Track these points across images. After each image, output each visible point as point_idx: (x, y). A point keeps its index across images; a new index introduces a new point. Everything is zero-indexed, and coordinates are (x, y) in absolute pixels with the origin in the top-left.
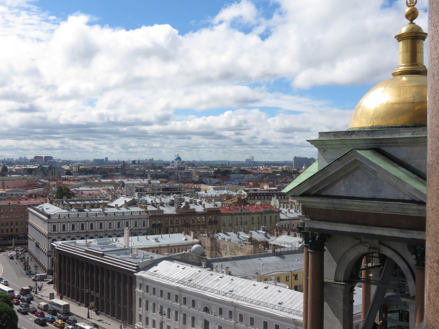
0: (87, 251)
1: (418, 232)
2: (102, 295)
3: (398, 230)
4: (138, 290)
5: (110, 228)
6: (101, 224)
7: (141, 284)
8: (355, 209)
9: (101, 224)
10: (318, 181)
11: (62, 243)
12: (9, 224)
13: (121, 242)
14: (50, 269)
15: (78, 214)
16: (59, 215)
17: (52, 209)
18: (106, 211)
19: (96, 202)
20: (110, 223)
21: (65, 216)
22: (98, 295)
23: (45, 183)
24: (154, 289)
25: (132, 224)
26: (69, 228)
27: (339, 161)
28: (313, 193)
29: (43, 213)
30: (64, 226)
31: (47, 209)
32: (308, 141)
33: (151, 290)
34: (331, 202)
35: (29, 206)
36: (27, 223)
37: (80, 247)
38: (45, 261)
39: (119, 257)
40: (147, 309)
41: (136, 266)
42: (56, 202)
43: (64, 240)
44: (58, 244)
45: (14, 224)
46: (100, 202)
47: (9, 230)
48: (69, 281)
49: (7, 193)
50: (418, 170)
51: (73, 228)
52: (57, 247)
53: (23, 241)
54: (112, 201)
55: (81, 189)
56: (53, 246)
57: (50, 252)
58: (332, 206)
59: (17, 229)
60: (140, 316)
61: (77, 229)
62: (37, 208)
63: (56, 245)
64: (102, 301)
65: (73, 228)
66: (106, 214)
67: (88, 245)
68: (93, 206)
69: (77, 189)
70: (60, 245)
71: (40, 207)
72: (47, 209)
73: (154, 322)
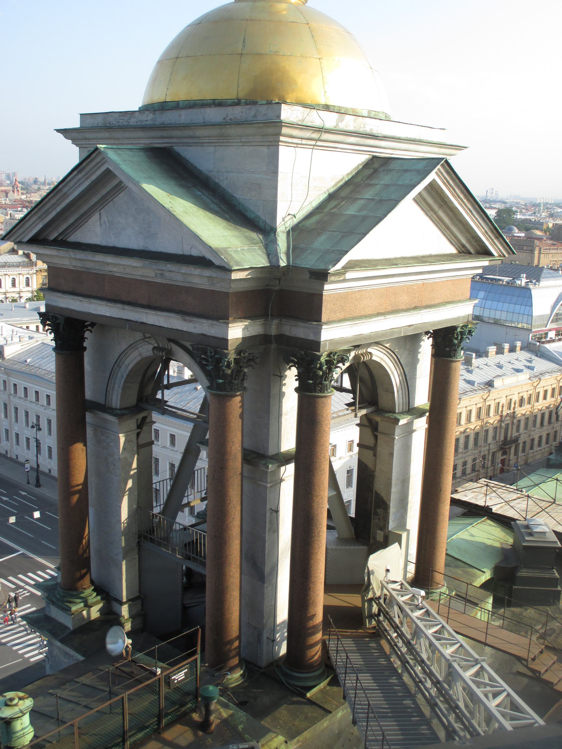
1: (210, 322)
3: (179, 317)
8: (117, 271)
10: (54, 214)
24: (26, 389)
27: (79, 172)
28: (52, 238)
32: (58, 131)
33: (21, 392)
34: (73, 256)
50: (232, 196)
58: (80, 265)
73: (28, 439)
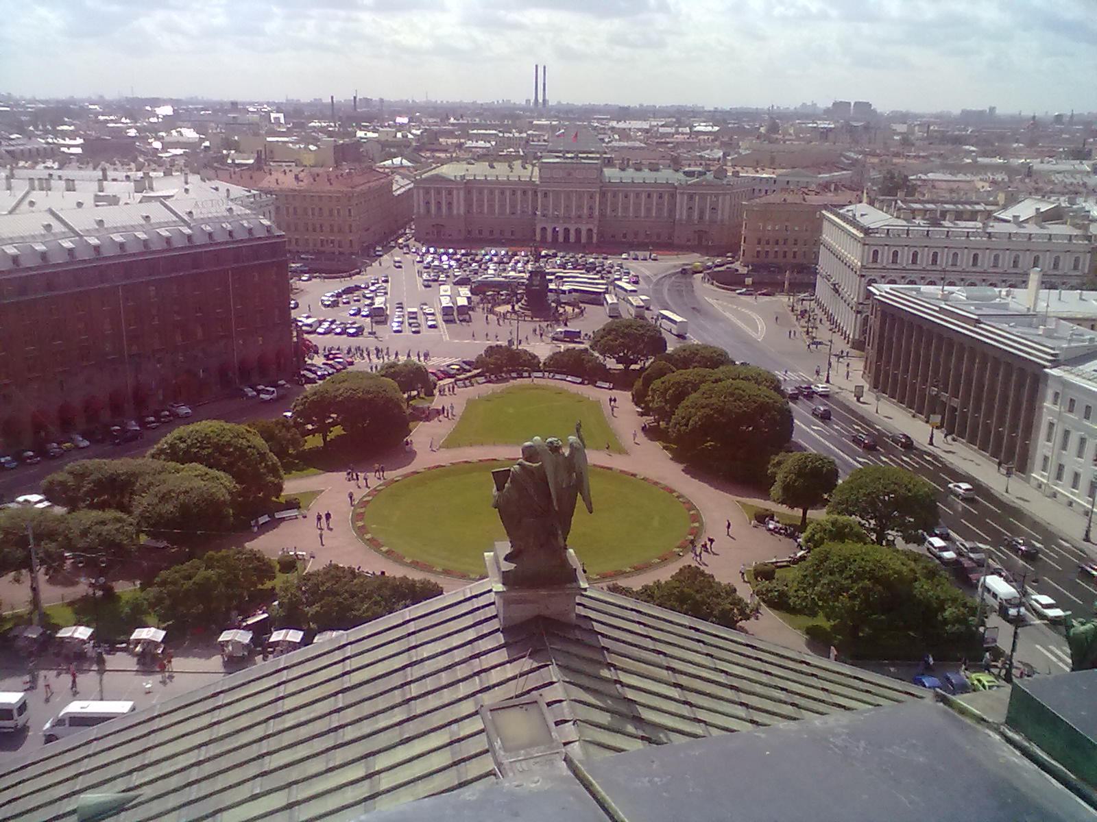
0: (942, 310)
2: (965, 404)
4: (1047, 404)
5: (995, 266)
6: (975, 257)
7: (1057, 395)
9: (975, 257)
11: (891, 289)
12: (781, 242)
13: (1020, 299)
14: (857, 337)
15: (928, 231)
16: (888, 230)
17: (875, 217)
18: (989, 230)
19: (968, 207)
20: (996, 257)
21: (900, 232)
22: (956, 402)
23: (857, 160)
25: (1047, 261)
26: (905, 258)
29: (853, 222)
30: (895, 254)
31: (862, 215)
35: (825, 207)
36: (817, 243)
37: (928, 299)
38: (849, 322)
39: (1014, 331)
40: (1064, 447)
41: (1052, 355)
42: (882, 201)
43: (894, 282)
44: (882, 290)
45: (791, 241)
46: (977, 207)
47: (781, 255)
48: (897, 366)
49: (781, 178)
51: (914, 261)
52: (880, 295)
53: (805, 278)
54: (1005, 207)
55: (931, 176)
56: (870, 295)
57: (861, 304)
59: (795, 253)
60: (1046, 459)
61: (922, 261)
62: (841, 211)
63: (877, 293)
64: (964, 415)
65: (914, 261)
66: (990, 235)
67: (945, 298)
68: (959, 216)
69: (924, 177)
70: (886, 292)
71: (848, 211)
72: (862, 215)
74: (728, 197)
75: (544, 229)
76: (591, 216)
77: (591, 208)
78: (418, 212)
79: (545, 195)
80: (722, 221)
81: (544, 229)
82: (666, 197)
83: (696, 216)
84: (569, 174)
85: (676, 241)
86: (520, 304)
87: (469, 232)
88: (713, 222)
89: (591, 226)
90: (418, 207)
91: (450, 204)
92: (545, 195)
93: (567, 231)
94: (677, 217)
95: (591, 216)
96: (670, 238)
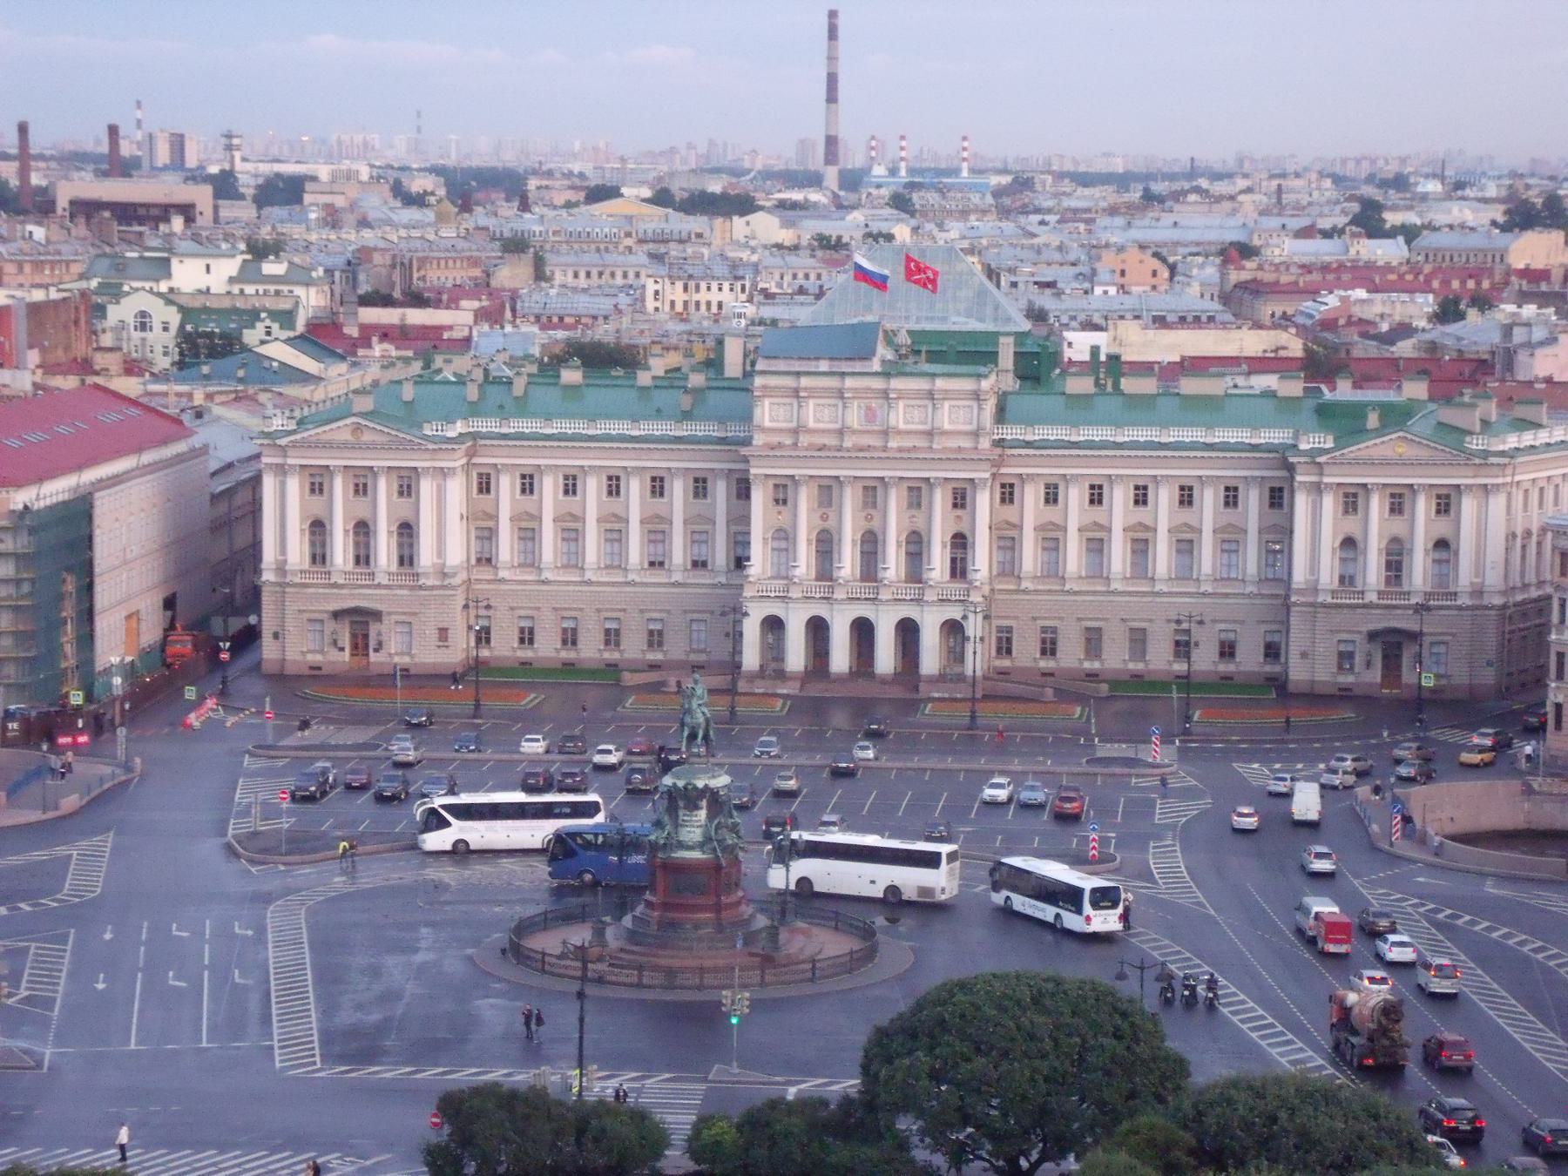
74: (1497, 503)
75: (774, 625)
76: (959, 569)
77: (960, 542)
78: (281, 569)
79: (782, 495)
80: (1478, 592)
81: (774, 625)
82: (1253, 500)
83: (1373, 572)
84: (870, 415)
85: (1298, 672)
86: (627, 921)
87: (484, 637)
88: (1443, 589)
89: (955, 613)
90: (282, 542)
91: (407, 531)
92: (782, 495)
93: (863, 631)
94: (1300, 576)
95: (959, 569)
96: (1272, 651)
